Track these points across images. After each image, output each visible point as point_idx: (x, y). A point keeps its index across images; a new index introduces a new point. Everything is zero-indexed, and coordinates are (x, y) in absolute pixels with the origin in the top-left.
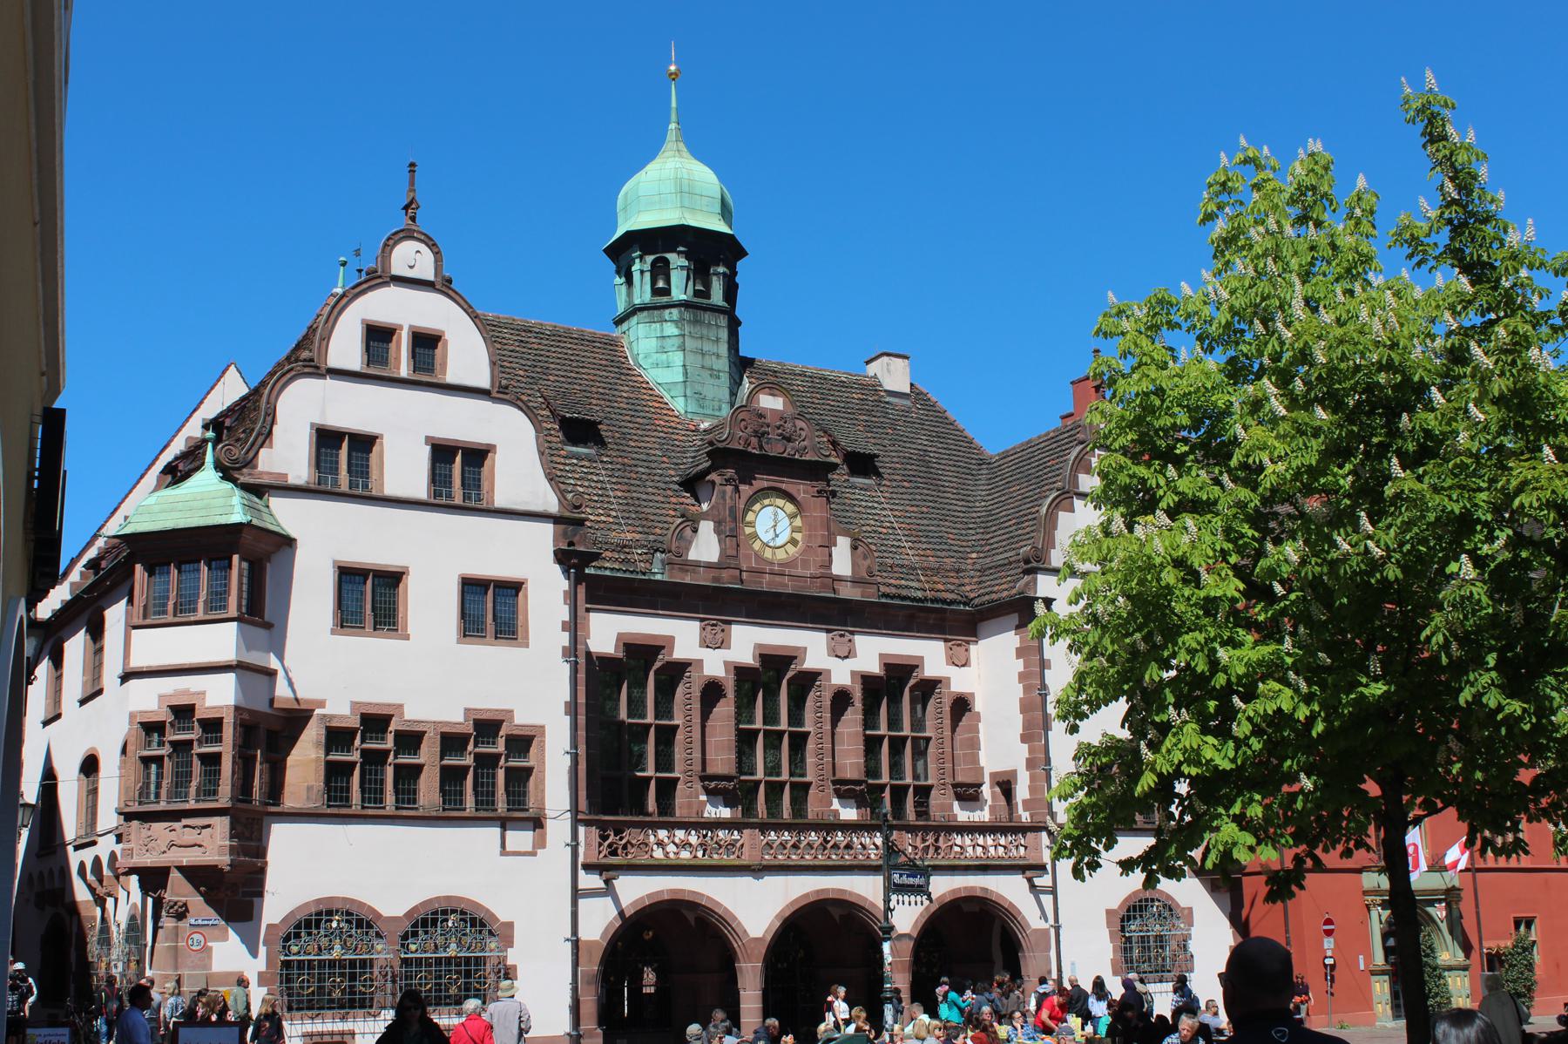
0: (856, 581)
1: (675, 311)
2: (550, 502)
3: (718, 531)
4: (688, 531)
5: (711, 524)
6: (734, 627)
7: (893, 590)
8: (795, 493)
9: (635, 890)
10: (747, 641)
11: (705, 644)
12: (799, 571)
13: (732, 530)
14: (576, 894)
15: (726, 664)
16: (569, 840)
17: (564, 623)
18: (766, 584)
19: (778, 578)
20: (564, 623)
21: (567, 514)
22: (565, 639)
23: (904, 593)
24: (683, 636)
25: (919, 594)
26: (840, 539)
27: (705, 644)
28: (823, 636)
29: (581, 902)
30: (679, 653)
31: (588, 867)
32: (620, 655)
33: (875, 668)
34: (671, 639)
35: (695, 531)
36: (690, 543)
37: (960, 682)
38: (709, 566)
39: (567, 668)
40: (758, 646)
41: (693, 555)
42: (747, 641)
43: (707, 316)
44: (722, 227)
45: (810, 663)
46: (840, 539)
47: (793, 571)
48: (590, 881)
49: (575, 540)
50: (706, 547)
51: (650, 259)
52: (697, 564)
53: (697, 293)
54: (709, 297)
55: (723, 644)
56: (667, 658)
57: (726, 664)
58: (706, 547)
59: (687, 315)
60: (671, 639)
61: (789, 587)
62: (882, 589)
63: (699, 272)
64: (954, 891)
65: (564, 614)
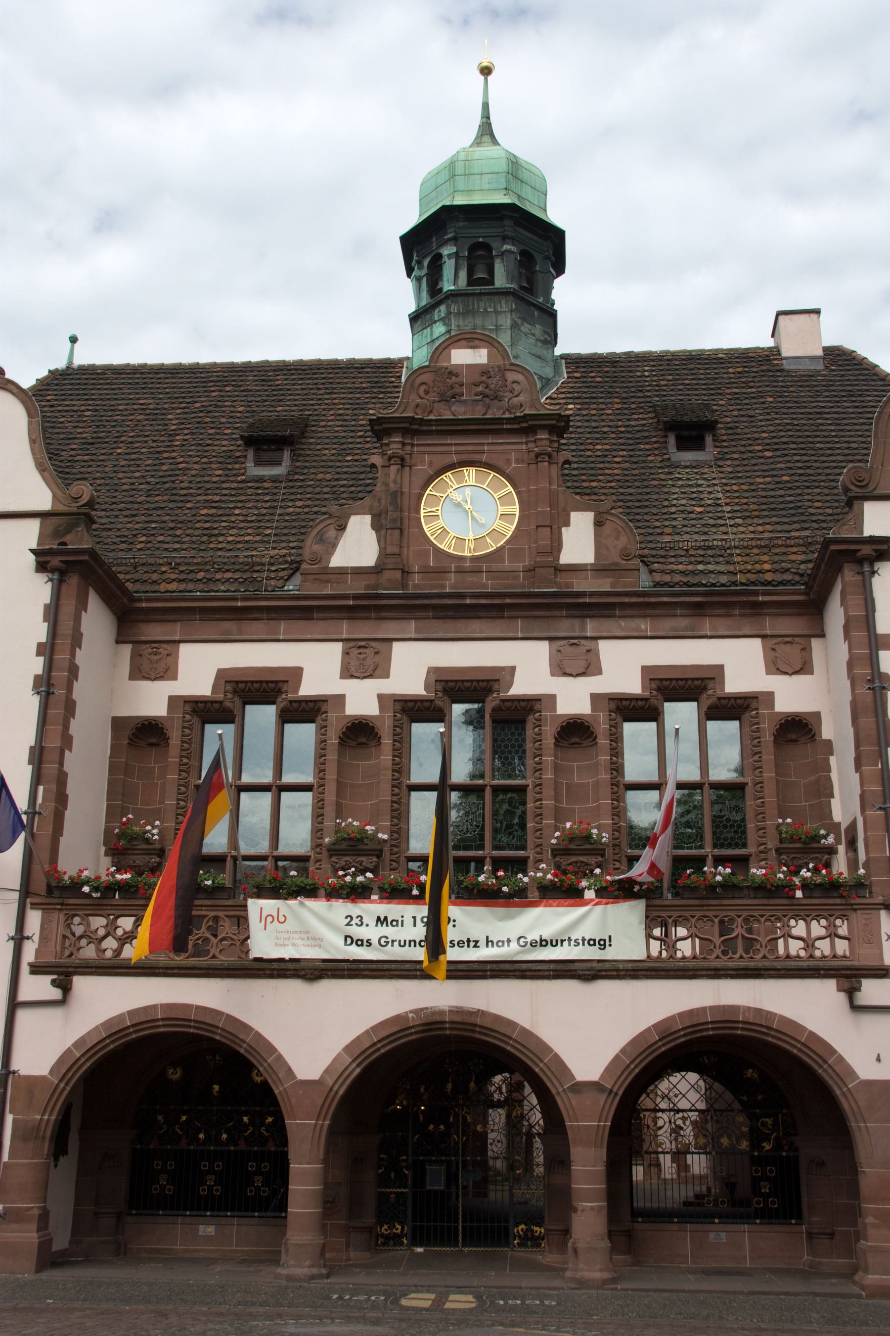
0: (599, 569)
1: (443, 308)
2: (42, 498)
3: (376, 526)
4: (332, 533)
5: (368, 519)
6: (396, 646)
7: (677, 578)
8: (501, 464)
9: (107, 1001)
10: (413, 665)
11: (347, 673)
12: (507, 565)
13: (397, 524)
14: (14, 1005)
15: (382, 698)
16: (12, 933)
17: (40, 645)
18: (450, 584)
19: (469, 578)
20: (40, 645)
21: (61, 508)
22: (38, 665)
23: (694, 580)
24: (317, 665)
25: (724, 579)
26: (575, 516)
27: (347, 673)
28: (542, 649)
29: (22, 1016)
30: (308, 689)
31: (36, 969)
32: (220, 697)
33: (633, 686)
34: (296, 673)
35: (342, 528)
36: (334, 546)
37: (791, 695)
38: (359, 572)
39: (34, 703)
40: (432, 671)
41: (337, 560)
42: (413, 665)
43: (482, 304)
44: (506, 200)
45: (520, 688)
46: (575, 516)
47: (495, 566)
48: (38, 987)
49: (67, 538)
50: (357, 545)
51: (426, 263)
52: (342, 572)
53: (471, 282)
54: (493, 284)
55: (379, 669)
56: (290, 696)
57: (381, 697)
58: (357, 545)
59: (454, 308)
60: (296, 673)
61: (488, 584)
62: (658, 577)
63: (478, 258)
64: (691, 1013)
65: (41, 633)
